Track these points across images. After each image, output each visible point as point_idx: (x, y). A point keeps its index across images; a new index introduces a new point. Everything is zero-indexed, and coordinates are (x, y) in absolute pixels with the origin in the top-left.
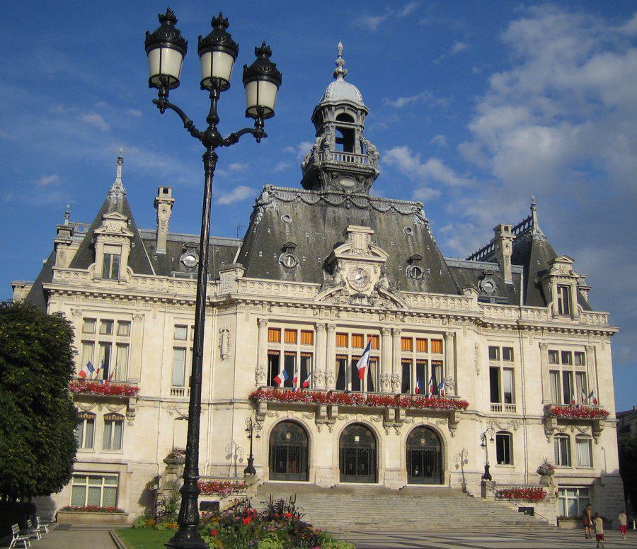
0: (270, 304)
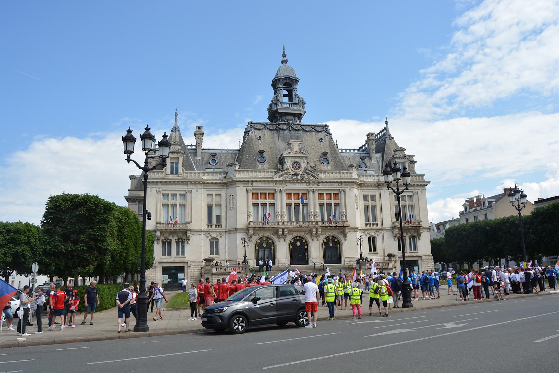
0: (252, 182)
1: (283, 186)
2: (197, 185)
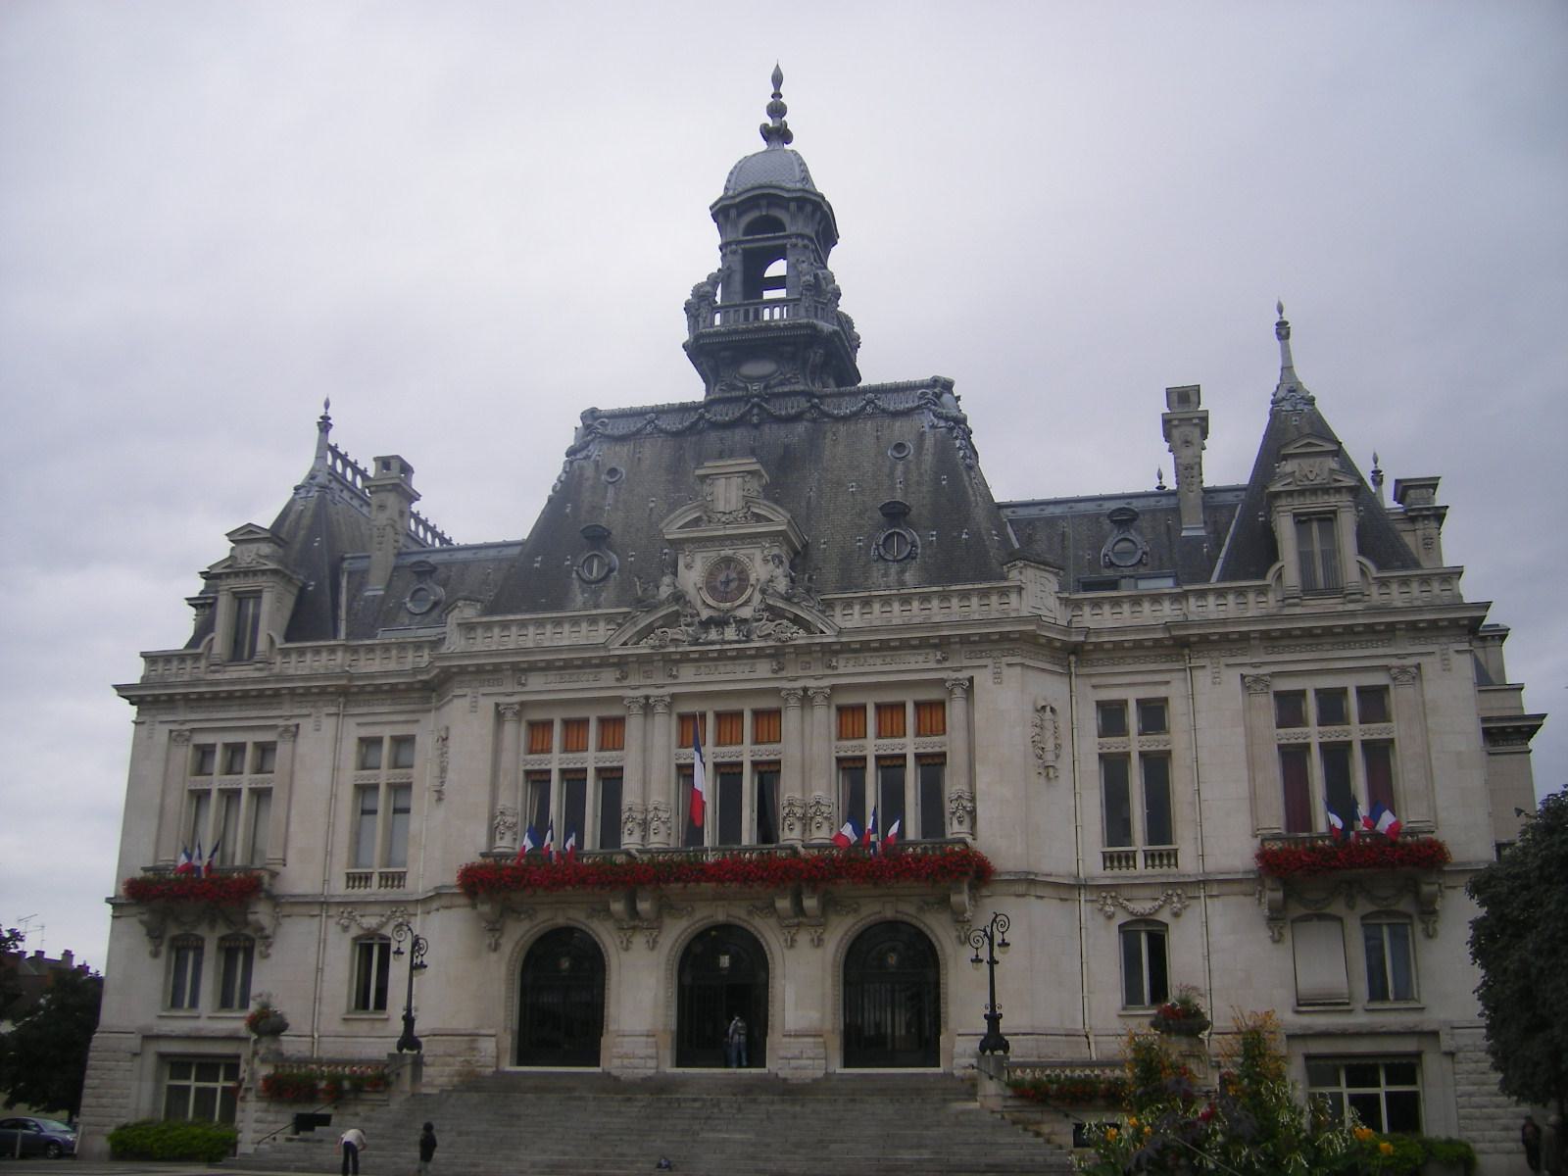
0: (521, 671)
1: (659, 682)
2: (321, 704)
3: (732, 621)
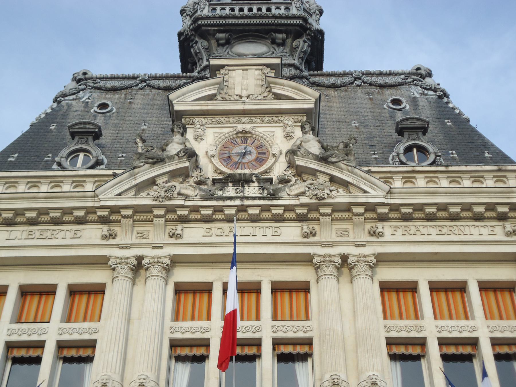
3: (254, 179)
